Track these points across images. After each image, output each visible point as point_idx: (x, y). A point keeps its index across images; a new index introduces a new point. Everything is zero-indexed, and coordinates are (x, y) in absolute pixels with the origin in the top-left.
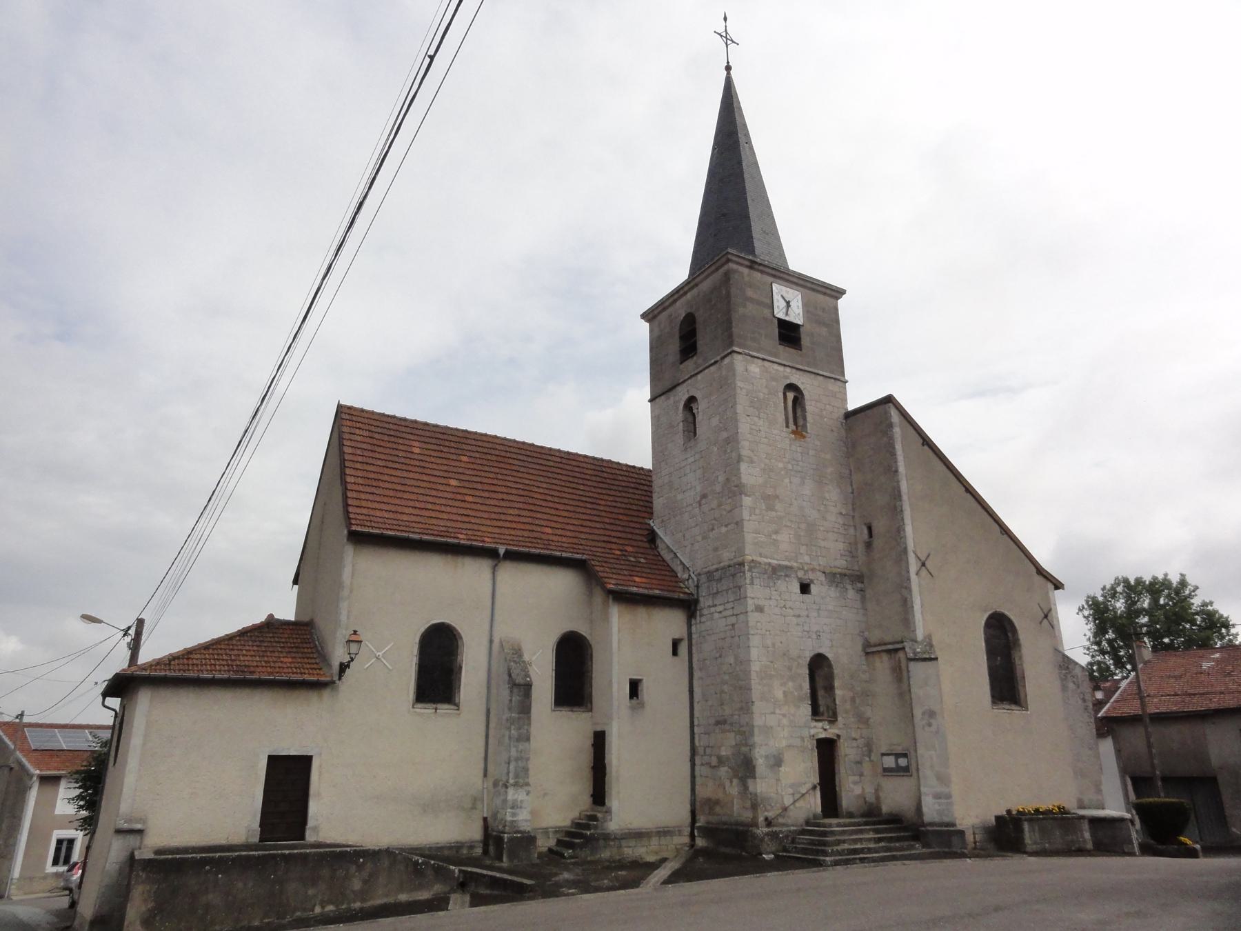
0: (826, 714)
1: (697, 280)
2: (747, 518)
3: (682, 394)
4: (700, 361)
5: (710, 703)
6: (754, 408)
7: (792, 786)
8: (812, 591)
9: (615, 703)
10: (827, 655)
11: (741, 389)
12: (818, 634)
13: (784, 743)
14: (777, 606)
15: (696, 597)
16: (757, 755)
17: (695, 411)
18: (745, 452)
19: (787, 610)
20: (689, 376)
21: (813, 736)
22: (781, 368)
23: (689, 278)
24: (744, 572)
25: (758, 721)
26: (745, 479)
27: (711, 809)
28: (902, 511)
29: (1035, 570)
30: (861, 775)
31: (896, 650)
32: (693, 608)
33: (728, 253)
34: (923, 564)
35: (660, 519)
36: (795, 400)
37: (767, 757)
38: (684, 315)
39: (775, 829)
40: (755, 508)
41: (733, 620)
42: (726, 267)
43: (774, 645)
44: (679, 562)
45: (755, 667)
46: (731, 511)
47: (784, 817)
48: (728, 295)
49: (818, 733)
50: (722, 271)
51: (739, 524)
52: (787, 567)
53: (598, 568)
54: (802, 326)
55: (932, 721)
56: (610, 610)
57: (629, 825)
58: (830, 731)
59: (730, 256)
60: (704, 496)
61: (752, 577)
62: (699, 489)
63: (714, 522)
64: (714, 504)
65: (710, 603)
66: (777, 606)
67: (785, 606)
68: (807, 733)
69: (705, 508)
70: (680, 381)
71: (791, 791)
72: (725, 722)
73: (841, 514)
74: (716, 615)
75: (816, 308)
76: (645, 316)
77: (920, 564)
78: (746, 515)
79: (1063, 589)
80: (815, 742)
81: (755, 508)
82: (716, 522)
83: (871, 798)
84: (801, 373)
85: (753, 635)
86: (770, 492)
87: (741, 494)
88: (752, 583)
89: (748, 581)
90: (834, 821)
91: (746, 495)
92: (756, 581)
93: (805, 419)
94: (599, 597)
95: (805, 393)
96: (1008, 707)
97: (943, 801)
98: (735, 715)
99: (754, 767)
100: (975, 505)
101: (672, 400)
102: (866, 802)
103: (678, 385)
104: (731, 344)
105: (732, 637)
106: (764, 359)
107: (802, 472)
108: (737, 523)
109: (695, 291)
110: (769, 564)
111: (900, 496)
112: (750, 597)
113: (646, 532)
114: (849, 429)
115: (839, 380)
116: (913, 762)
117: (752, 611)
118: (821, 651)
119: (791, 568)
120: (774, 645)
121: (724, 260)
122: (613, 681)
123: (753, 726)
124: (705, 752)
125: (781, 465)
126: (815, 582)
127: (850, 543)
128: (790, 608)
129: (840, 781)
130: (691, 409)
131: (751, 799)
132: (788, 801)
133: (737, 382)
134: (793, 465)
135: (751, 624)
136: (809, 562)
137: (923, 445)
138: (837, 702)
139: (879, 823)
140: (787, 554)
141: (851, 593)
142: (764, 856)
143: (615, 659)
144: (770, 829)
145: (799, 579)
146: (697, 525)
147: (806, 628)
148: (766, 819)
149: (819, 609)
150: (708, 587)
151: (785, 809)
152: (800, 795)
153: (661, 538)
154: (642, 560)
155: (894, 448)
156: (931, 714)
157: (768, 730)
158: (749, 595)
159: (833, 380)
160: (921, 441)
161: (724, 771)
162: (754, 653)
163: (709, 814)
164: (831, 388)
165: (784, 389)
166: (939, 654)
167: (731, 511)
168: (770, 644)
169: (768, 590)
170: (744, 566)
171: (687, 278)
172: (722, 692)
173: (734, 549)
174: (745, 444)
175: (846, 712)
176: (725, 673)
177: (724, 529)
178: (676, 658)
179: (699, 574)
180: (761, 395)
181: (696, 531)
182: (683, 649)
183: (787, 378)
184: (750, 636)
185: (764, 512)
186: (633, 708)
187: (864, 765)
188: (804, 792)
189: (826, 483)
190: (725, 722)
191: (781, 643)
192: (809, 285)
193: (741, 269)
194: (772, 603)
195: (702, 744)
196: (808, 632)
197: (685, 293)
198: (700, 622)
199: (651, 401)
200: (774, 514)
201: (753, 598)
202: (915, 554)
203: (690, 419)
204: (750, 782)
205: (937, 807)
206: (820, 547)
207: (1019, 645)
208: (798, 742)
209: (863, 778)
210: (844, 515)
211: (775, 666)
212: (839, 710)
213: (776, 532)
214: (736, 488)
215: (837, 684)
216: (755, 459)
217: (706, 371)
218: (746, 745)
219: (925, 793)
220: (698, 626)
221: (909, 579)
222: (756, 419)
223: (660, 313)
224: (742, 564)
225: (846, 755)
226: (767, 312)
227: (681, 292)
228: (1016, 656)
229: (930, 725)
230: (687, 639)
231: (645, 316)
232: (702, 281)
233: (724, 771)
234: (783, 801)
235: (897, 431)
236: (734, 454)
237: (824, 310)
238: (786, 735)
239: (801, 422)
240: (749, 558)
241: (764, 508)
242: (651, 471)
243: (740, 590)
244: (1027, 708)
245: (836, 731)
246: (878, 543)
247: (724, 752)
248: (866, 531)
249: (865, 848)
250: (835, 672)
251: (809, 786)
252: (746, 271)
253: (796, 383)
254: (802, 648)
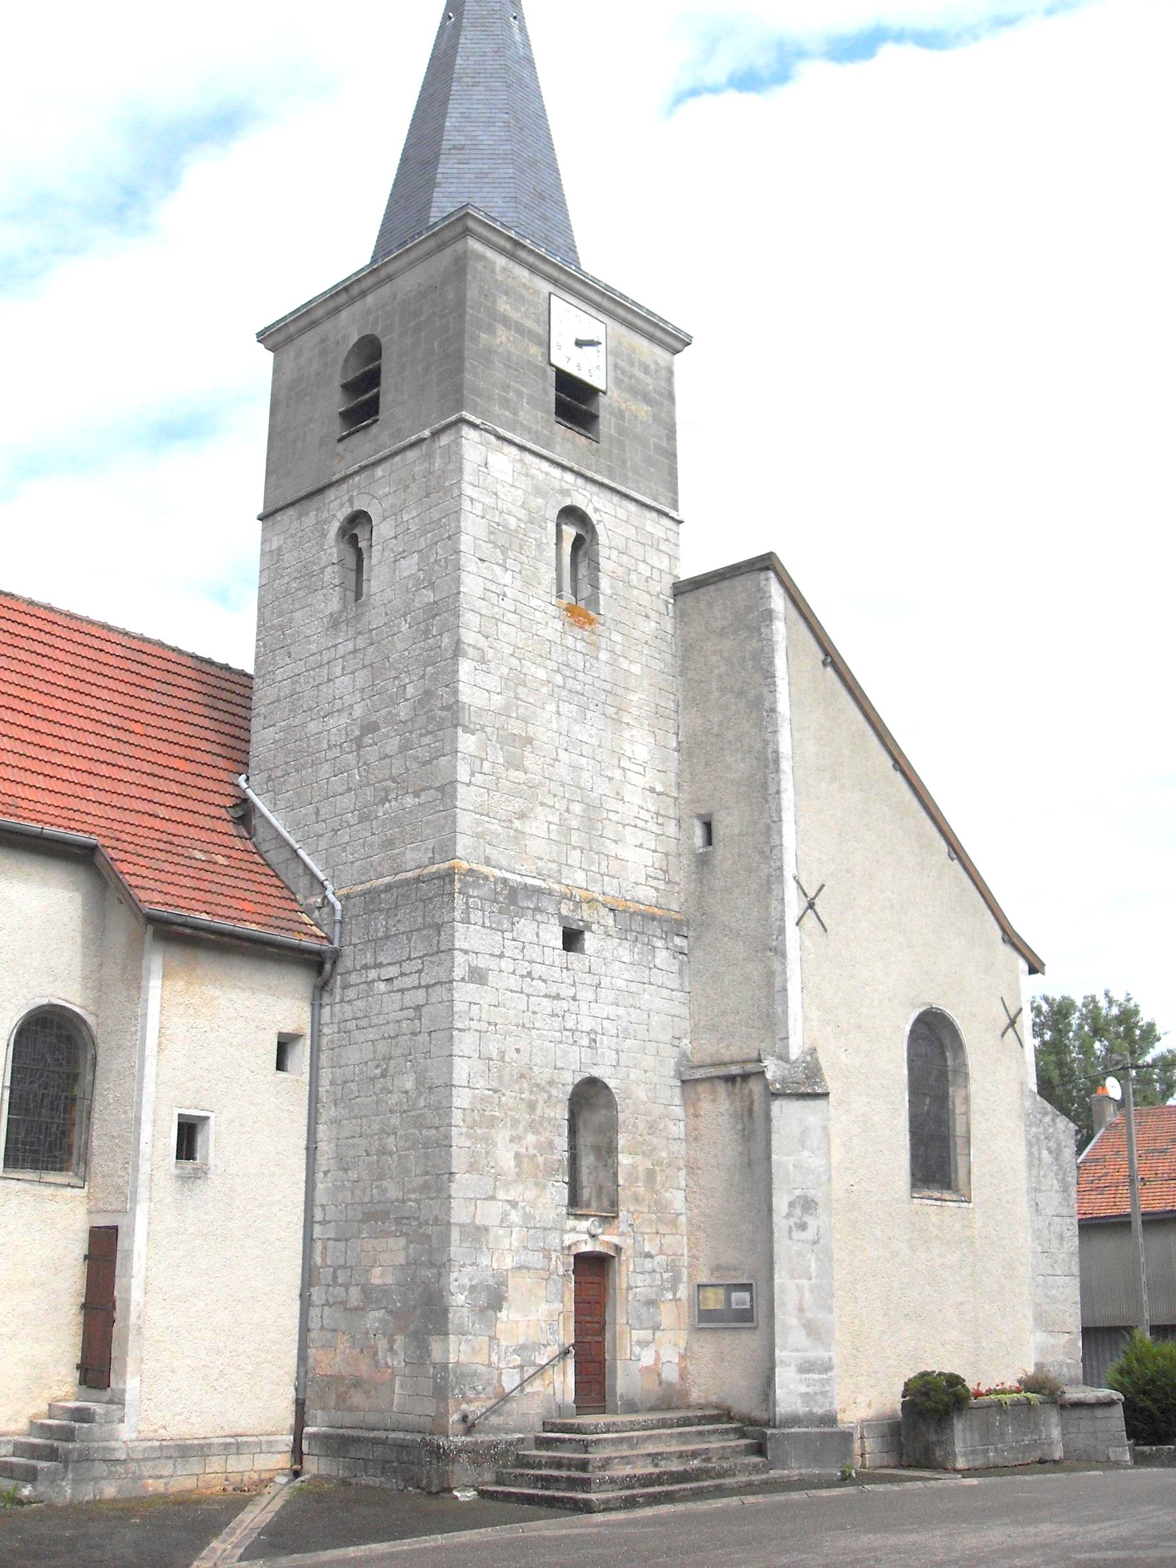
0: (594, 1204)
1: (391, 269)
2: (466, 779)
3: (337, 509)
4: (384, 438)
5: (353, 1175)
6: (496, 546)
7: (521, 1349)
8: (586, 945)
9: (145, 1168)
10: (607, 1081)
11: (472, 500)
12: (593, 1036)
13: (508, 1262)
14: (514, 973)
15: (336, 945)
16: (453, 1287)
17: (362, 544)
18: (469, 637)
19: (535, 982)
20: (356, 467)
21: (569, 1247)
22: (556, 472)
23: (374, 260)
24: (452, 894)
25: (460, 1213)
26: (466, 694)
27: (342, 1398)
28: (778, 792)
29: (998, 933)
30: (656, 1328)
31: (745, 1077)
32: (328, 967)
33: (468, 214)
34: (811, 906)
35: (265, 775)
36: (578, 542)
37: (473, 1289)
38: (355, 338)
39: (480, 1437)
40: (482, 760)
41: (412, 998)
42: (459, 246)
43: (502, 1054)
44: (301, 871)
45: (461, 1099)
46: (430, 762)
47: (500, 1415)
48: (461, 301)
49: (576, 1243)
50: (448, 253)
51: (447, 790)
52: (539, 891)
53: (124, 867)
54: (605, 393)
55: (810, 1221)
56: (145, 961)
57: (162, 1431)
58: (601, 1237)
59: (471, 224)
60: (370, 728)
61: (468, 907)
62: (358, 711)
63: (390, 783)
64: (392, 745)
65: (369, 959)
66: (514, 973)
67: (529, 974)
68: (557, 1241)
69: (371, 754)
70: (334, 478)
71: (517, 1360)
72: (384, 1216)
73: (652, 790)
74: (382, 987)
75: (632, 364)
76: (264, 337)
77: (805, 905)
78: (463, 774)
79: (1043, 973)
80: (572, 1259)
81: (482, 760)
82: (394, 785)
83: (671, 1374)
84: (595, 489)
85: (460, 1030)
86: (515, 727)
87: (455, 726)
88: (466, 921)
89: (457, 915)
90: (602, 1419)
91: (466, 730)
92: (475, 916)
93: (595, 586)
94: (120, 928)
95: (599, 529)
96: (937, 1195)
97: (816, 1376)
98: (410, 1200)
99: (446, 1311)
100: (909, 795)
101: (310, 520)
102: (661, 1383)
103: (330, 485)
104: (459, 405)
105: (414, 1034)
106: (522, 448)
107: (583, 695)
108: (441, 789)
109: (386, 290)
110: (505, 881)
111: (777, 761)
112: (461, 950)
113: (229, 802)
114: (681, 617)
115: (666, 515)
116: (761, 1302)
117: (463, 980)
118: (596, 1072)
119: (550, 893)
120: (502, 1054)
121: (459, 229)
122: (143, 1117)
123: (449, 1224)
124: (335, 1277)
125: (541, 674)
126: (595, 927)
127: (667, 855)
128: (540, 978)
129: (614, 1338)
130: (354, 540)
131: (434, 1377)
132: (510, 1381)
133: (464, 485)
134: (565, 677)
135: (459, 1007)
136: (584, 885)
137: (824, 664)
138: (621, 1181)
139: (687, 1422)
140: (540, 864)
141: (662, 957)
142: (456, 1493)
143: (150, 1069)
144: (469, 1439)
145: (561, 918)
146: (349, 790)
147: (570, 1024)
148: (464, 1418)
149: (598, 986)
150: (367, 927)
151: (505, 1398)
152: (537, 1369)
153: (263, 816)
154: (221, 860)
155: (771, 663)
156: (808, 1204)
157: (477, 1233)
158: (457, 945)
159: (654, 514)
160: (821, 656)
161: (374, 1318)
162: (461, 1070)
163: (337, 1408)
164: (649, 528)
165: (559, 516)
166: (832, 1084)
167: (430, 762)
168: (495, 1055)
169: (498, 937)
170: (452, 882)
171: (367, 261)
172: (383, 1151)
173: (430, 844)
174: (469, 619)
175: (637, 1199)
176: (391, 1112)
177: (410, 801)
178: (281, 1074)
179: (348, 897)
180: (513, 523)
181: (347, 801)
182: (300, 1056)
183: (565, 493)
184: (455, 1033)
185: (501, 769)
186: (183, 1179)
187: (662, 1306)
188: (544, 1362)
189: (628, 724)
190: (384, 1216)
191: (518, 1051)
192: (621, 312)
193: (490, 254)
194: (505, 964)
195: (329, 1262)
196: (573, 1031)
197: (363, 294)
198: (342, 1001)
199: (261, 518)
200: (519, 776)
201: (466, 952)
202: (798, 882)
203: (351, 562)
204: (436, 1346)
205: (803, 1389)
206: (608, 856)
207: (966, 1076)
208: (535, 1259)
209: (658, 1334)
210: (659, 794)
211: (503, 1099)
212: (623, 1194)
213: (522, 816)
214: (444, 714)
215: (622, 1141)
216: (490, 654)
217: (398, 458)
218: (432, 1264)
219: (781, 1362)
220: (337, 1007)
221: (782, 930)
222: (498, 569)
223: (302, 332)
224: (448, 876)
225: (630, 1288)
226: (535, 351)
227: (355, 290)
228: (956, 1095)
229: (803, 1227)
230: (308, 1036)
231: (264, 337)
232: (403, 270)
233: (374, 1318)
234: (500, 1381)
235: (779, 628)
236: (446, 640)
237: (646, 369)
238: (515, 1244)
239: (585, 590)
240: (465, 865)
241: (501, 760)
242: (250, 677)
243: (439, 935)
244: (970, 1198)
245: (615, 1240)
246: (722, 853)
247: (377, 1277)
248: (699, 832)
249: (665, 1473)
250: (621, 1117)
251: (555, 1350)
252: (501, 261)
253: (583, 507)
254: (559, 1064)
